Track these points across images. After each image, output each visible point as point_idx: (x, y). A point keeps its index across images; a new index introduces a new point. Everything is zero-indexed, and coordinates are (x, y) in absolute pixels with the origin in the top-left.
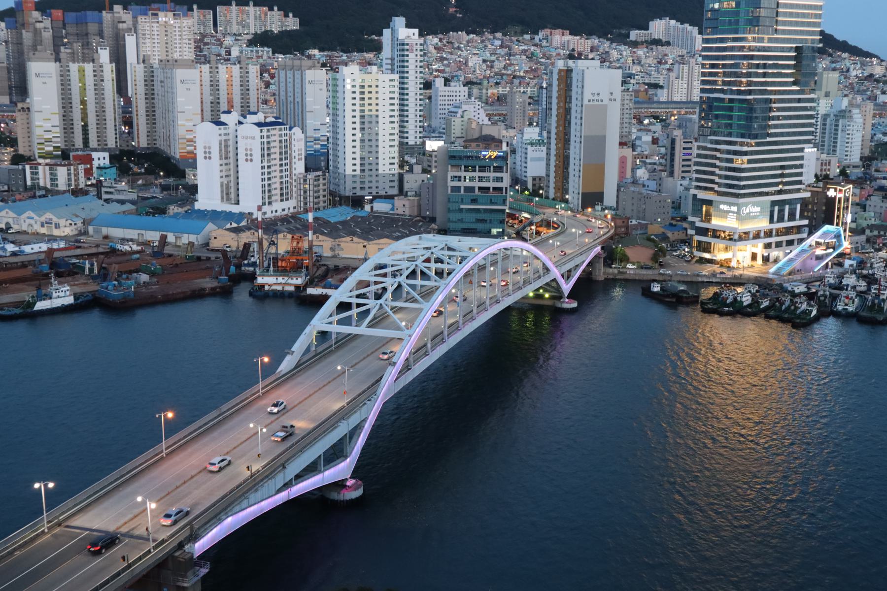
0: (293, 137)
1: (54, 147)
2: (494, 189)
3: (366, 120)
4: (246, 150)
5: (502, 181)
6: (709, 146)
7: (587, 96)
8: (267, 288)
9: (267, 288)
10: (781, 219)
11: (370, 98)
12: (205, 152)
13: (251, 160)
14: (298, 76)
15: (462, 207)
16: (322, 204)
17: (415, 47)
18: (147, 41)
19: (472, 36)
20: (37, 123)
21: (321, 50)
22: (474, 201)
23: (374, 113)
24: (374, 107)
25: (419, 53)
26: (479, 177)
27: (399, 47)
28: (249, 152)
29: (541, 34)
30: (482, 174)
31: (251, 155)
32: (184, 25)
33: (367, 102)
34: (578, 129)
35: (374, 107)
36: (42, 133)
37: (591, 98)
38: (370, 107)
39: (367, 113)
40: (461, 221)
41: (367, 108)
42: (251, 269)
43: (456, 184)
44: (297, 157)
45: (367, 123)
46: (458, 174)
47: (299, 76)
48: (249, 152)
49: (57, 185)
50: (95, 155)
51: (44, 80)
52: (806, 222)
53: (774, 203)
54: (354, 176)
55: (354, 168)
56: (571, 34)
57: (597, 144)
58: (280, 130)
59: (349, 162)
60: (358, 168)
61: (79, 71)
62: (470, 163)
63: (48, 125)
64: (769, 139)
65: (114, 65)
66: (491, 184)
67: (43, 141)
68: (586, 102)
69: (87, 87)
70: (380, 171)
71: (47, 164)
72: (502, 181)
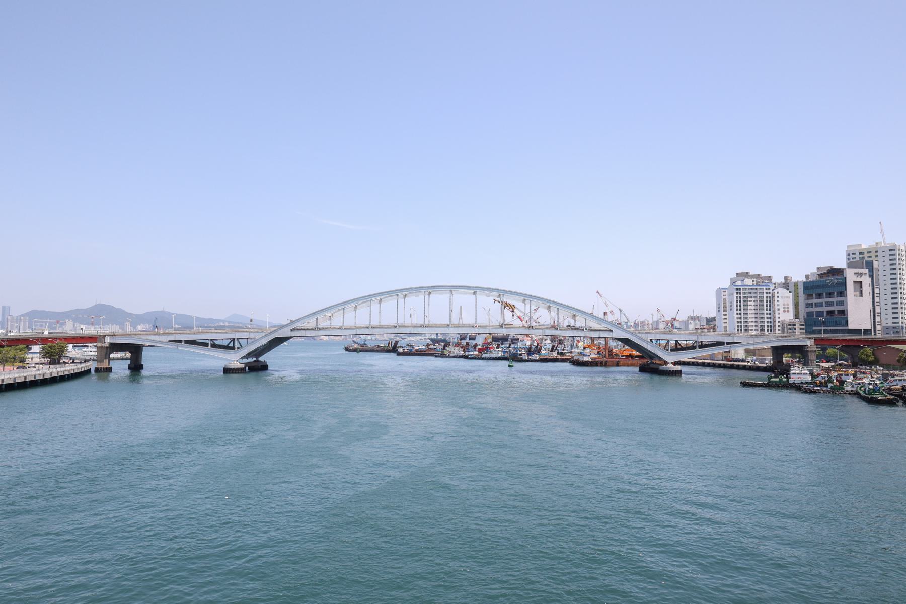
0: (776, 295)
2: (838, 311)
5: (843, 305)
15: (814, 328)
26: (826, 302)
43: (810, 310)
61: (794, 286)
62: (819, 291)
72: (843, 305)
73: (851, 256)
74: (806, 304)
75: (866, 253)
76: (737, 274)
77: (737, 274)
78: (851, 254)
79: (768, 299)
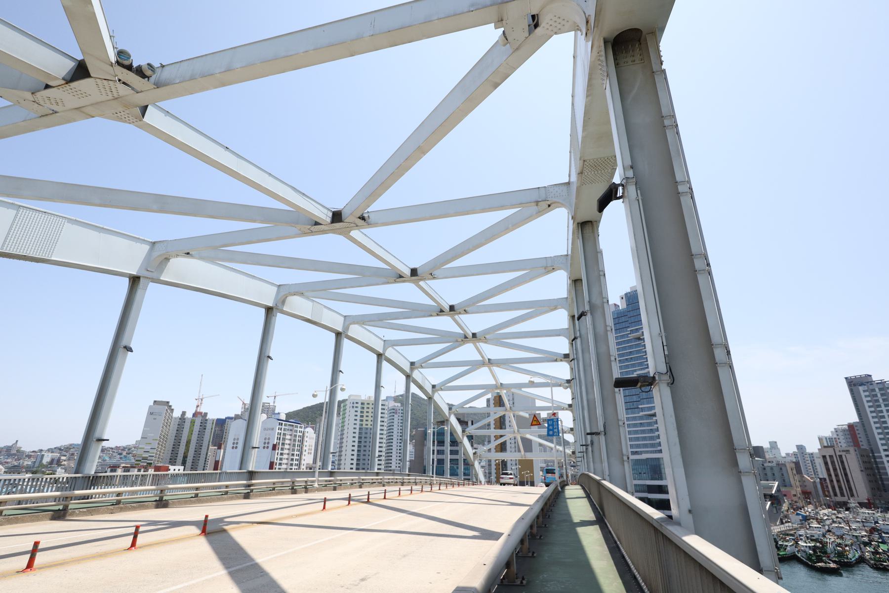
0: (306, 434)
1: (148, 463)
3: (364, 431)
11: (367, 416)
12: (234, 443)
17: (398, 411)
25: (400, 415)
32: (270, 410)
33: (365, 418)
36: (142, 453)
38: (367, 423)
39: (364, 426)
41: (364, 423)
44: (307, 451)
48: (267, 441)
51: (155, 417)
58: (297, 427)
61: (191, 422)
67: (140, 459)
69: (194, 432)
73: (355, 405)
74: (518, 452)
75: (366, 404)
76: (155, 401)
77: (155, 401)
78: (355, 403)
79: (279, 436)
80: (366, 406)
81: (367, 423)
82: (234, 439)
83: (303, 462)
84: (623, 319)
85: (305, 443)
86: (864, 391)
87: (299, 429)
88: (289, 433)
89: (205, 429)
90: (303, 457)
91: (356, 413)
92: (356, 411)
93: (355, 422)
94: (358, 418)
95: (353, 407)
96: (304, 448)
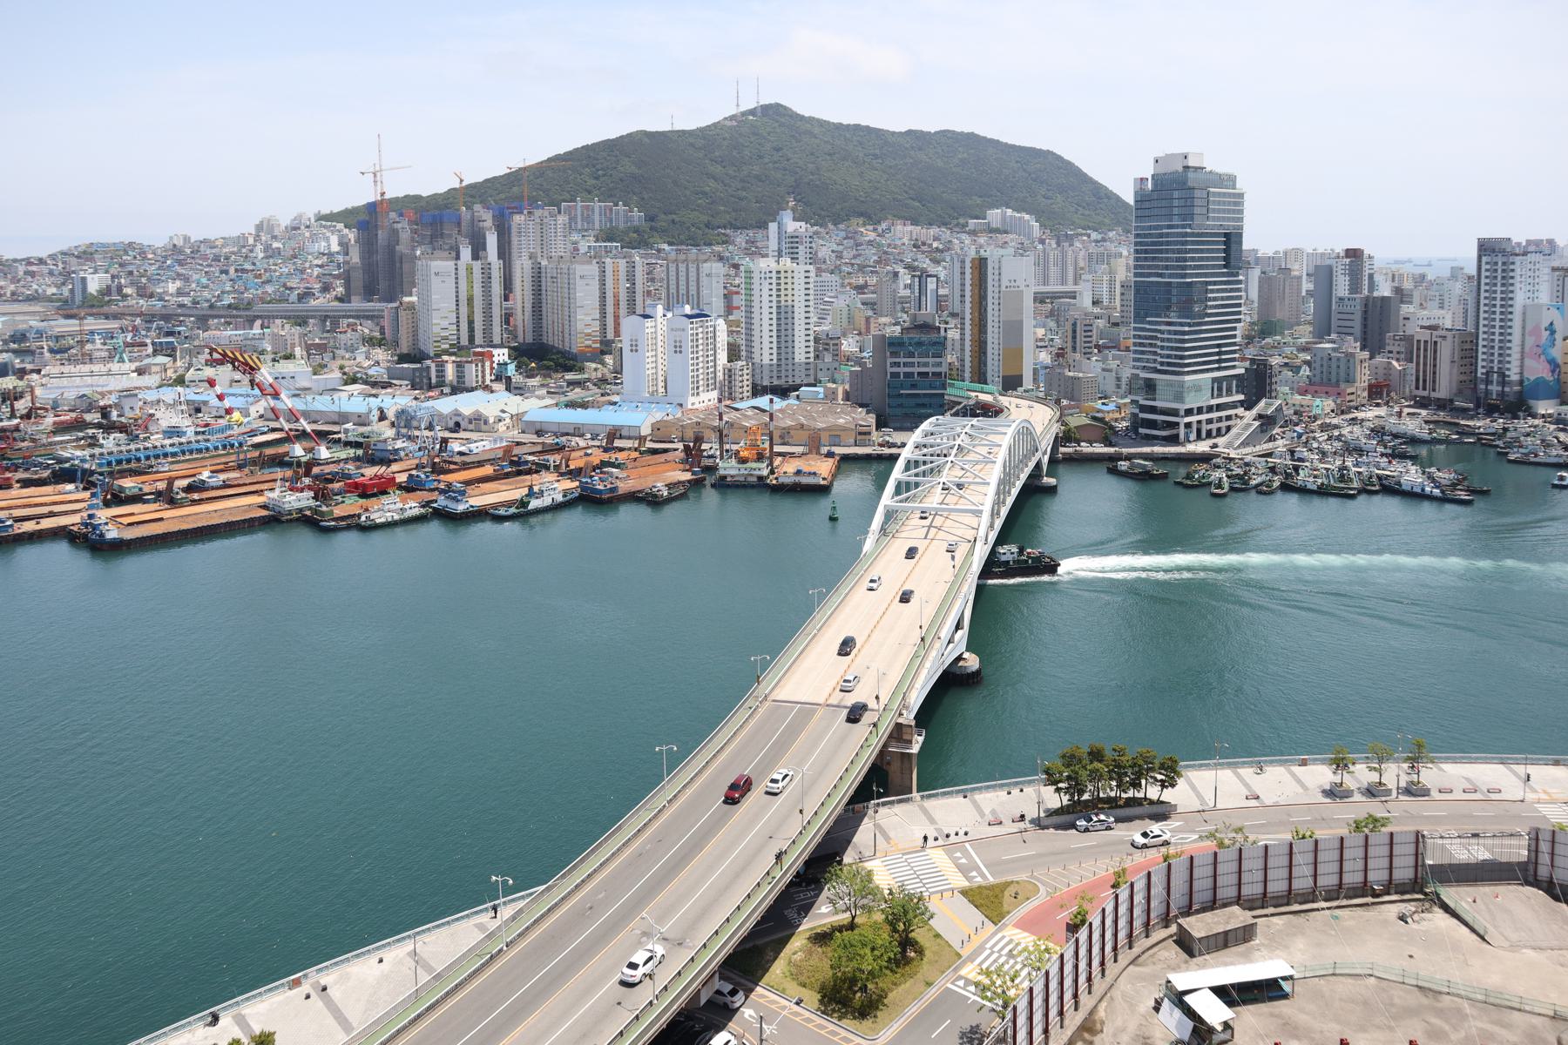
0: (718, 328)
2: (933, 373)
3: (783, 310)
4: (675, 342)
6: (1148, 327)
7: (1005, 283)
8: (729, 479)
9: (729, 479)
10: (1220, 396)
12: (631, 345)
13: (681, 352)
14: (693, 270)
16: (745, 394)
18: (523, 238)
19: (815, 228)
20: (434, 321)
21: (670, 244)
22: (914, 386)
23: (790, 303)
24: (790, 298)
25: (808, 245)
27: (788, 240)
28: (678, 344)
29: (884, 225)
30: (920, 360)
31: (680, 347)
34: (996, 314)
35: (790, 298)
37: (1008, 284)
38: (786, 298)
39: (783, 303)
40: (901, 406)
42: (711, 460)
43: (895, 370)
45: (784, 317)
46: (897, 360)
47: (674, 269)
48: (678, 344)
49: (464, 383)
50: (496, 352)
52: (1241, 397)
53: (1214, 380)
54: (771, 365)
55: (771, 357)
56: (912, 224)
57: (1014, 330)
59: (766, 352)
60: (775, 357)
63: (445, 323)
64: (1207, 319)
65: (501, 262)
66: (930, 370)
68: (1003, 288)
70: (797, 360)
71: (454, 362)
80: (782, 275)
81: (786, 298)
82: (631, 340)
83: (718, 362)
84: (1147, 205)
85: (718, 339)
86: (1487, 263)
87: (710, 324)
88: (700, 330)
89: (490, 278)
90: (718, 356)
91: (771, 287)
92: (771, 284)
93: (771, 299)
94: (774, 293)
95: (765, 278)
96: (718, 345)
